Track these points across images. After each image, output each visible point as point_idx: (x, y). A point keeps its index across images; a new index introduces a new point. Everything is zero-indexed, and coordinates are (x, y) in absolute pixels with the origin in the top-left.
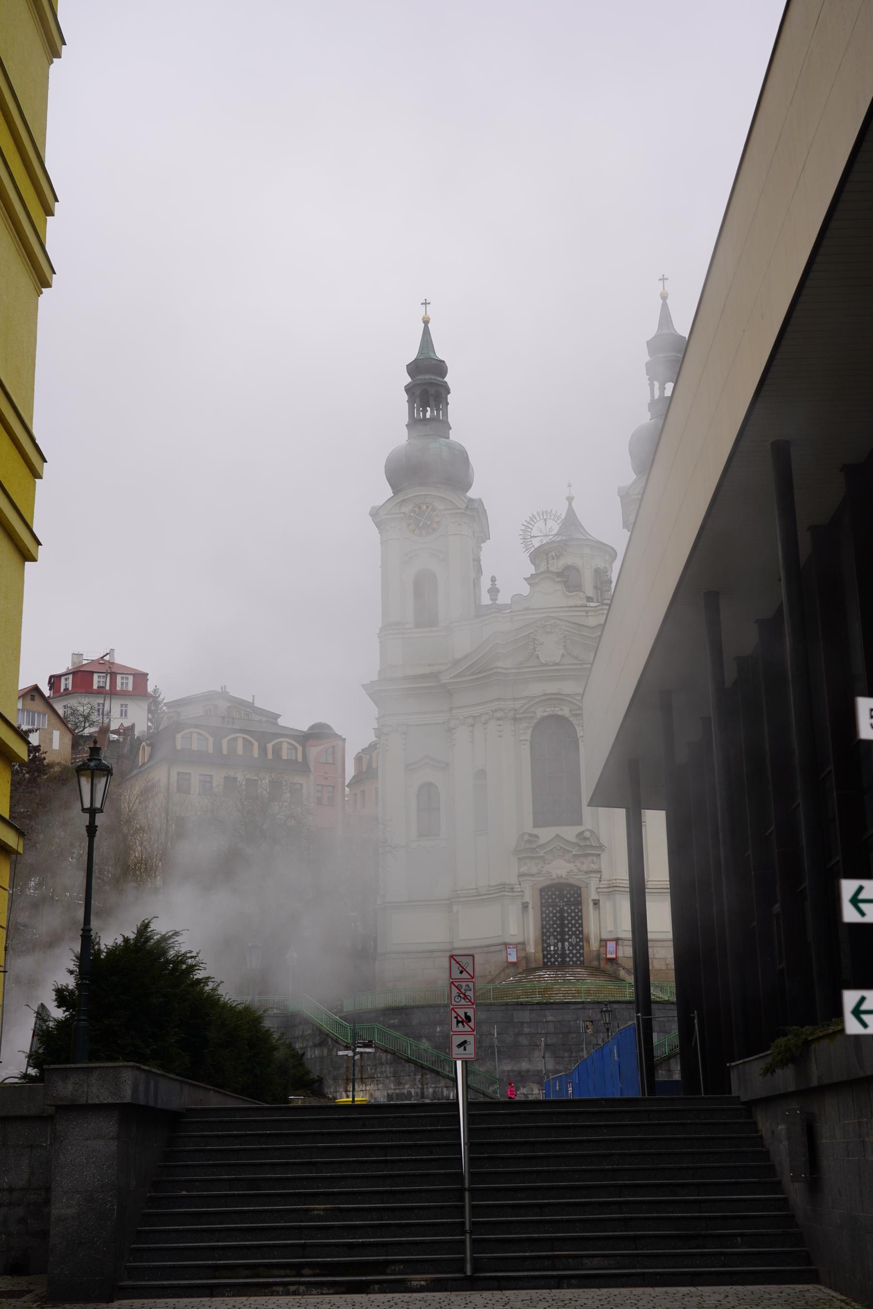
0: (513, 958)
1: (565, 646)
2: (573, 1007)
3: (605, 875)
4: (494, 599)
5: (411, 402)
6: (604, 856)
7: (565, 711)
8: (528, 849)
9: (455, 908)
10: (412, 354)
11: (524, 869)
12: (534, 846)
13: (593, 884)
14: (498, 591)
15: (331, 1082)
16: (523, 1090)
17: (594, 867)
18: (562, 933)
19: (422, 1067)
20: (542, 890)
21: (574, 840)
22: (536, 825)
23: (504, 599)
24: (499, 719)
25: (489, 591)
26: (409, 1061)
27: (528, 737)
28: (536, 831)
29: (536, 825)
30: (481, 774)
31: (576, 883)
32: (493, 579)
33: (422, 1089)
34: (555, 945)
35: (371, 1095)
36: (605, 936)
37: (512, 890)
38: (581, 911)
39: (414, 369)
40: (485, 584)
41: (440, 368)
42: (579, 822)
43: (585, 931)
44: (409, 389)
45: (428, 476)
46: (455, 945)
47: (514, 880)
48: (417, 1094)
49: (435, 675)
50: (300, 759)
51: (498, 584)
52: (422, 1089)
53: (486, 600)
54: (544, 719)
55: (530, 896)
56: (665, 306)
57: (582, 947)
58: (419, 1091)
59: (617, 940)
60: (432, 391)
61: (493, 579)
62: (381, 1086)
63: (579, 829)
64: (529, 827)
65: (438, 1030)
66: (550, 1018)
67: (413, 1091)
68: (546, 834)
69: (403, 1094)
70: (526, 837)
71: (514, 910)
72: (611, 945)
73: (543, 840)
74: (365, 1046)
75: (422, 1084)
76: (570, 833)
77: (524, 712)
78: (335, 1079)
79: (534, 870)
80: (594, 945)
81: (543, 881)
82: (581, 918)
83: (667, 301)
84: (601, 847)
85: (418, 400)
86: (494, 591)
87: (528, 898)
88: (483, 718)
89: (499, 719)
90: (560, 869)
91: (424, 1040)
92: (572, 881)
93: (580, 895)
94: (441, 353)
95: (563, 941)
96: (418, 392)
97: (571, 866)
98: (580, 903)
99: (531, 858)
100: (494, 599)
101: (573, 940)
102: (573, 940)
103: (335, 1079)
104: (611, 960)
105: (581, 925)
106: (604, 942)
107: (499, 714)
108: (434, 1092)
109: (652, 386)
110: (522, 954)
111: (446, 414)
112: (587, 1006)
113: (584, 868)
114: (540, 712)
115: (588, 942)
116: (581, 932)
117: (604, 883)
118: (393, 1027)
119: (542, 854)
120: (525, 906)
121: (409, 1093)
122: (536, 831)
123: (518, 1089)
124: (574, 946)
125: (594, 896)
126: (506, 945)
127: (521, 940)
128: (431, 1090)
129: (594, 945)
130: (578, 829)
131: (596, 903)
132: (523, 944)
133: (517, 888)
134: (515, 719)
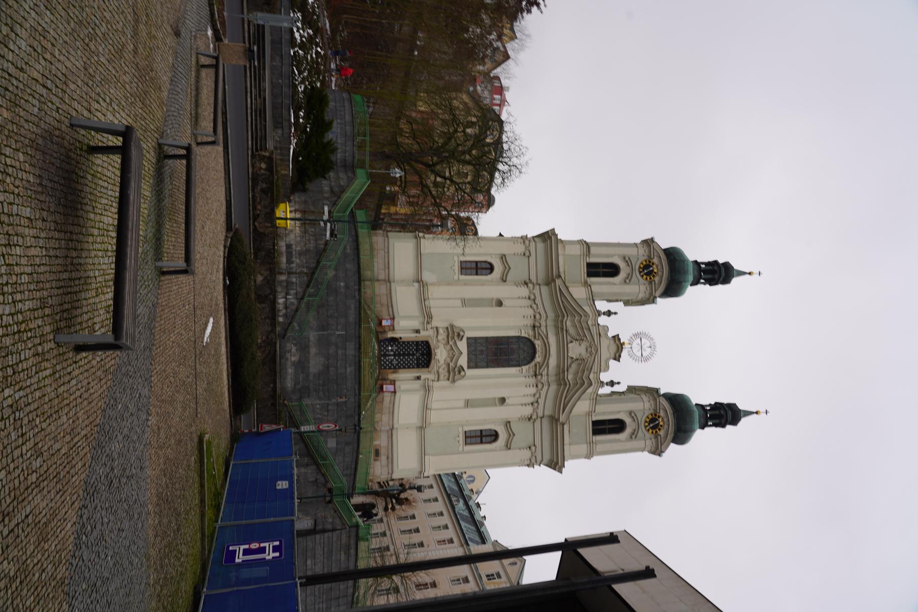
0: (384, 323)
1: (577, 359)
2: (357, 387)
3: (436, 384)
4: (604, 313)
5: (708, 264)
6: (447, 383)
7: (538, 359)
8: (454, 333)
9: (416, 285)
10: (737, 266)
11: (441, 331)
12: (456, 338)
13: (431, 376)
14: (609, 316)
15: (303, 198)
16: (294, 349)
17: (442, 377)
18: (399, 355)
19: (313, 273)
20: (427, 342)
21: (458, 364)
22: (468, 339)
23: (603, 320)
24: (535, 317)
25: (609, 311)
26: (318, 262)
27: (523, 335)
28: (465, 339)
29: (468, 339)
30: (500, 303)
31: (431, 365)
32: (615, 313)
33: (296, 273)
34: (392, 350)
35: (291, 231)
36: (397, 383)
37: (428, 323)
38: (413, 367)
39: (727, 267)
40: (612, 306)
41: (726, 280)
42: (469, 367)
43: (401, 371)
44: (716, 262)
45: (670, 273)
46: (392, 284)
47: (435, 323)
48: (291, 268)
49: (559, 276)
51: (613, 316)
52: (296, 273)
53: (602, 306)
55: (424, 335)
56: (751, 413)
57: (390, 368)
58: (294, 270)
59: (395, 392)
60: (716, 276)
61: (615, 313)
62: (299, 239)
63: (465, 367)
64: (469, 334)
65: (342, 284)
66: (348, 370)
67: (294, 265)
68: (463, 346)
69: (292, 257)
70: (462, 333)
71: (416, 324)
72: (391, 388)
73: (459, 343)
74: (332, 232)
75: (299, 273)
76: (463, 361)
77: (539, 334)
78: (305, 202)
79: (440, 338)
80: (392, 376)
81: (433, 344)
82: (409, 367)
83: (755, 415)
84: (454, 381)
85: (711, 268)
86: (609, 313)
87: (423, 333)
88: (534, 306)
89: (535, 317)
90: (441, 354)
91: (334, 273)
92: (433, 362)
93: (423, 367)
94: (735, 281)
95: (394, 355)
96: (716, 268)
97: (442, 362)
98: (418, 367)
99: (448, 336)
100: (604, 313)
101: (395, 362)
102: (395, 362)
103: (305, 202)
104: (382, 388)
105: (404, 368)
106: (393, 382)
107: (538, 316)
108: (293, 283)
109: (710, 405)
110: (387, 329)
112: (357, 398)
113: (441, 370)
114: (538, 343)
115: (394, 372)
116: (400, 368)
117: (431, 383)
118: (345, 248)
119: (451, 343)
120: (418, 331)
121: (292, 262)
122: (465, 339)
123: (295, 345)
124: (391, 363)
125: (423, 377)
126: (393, 319)
127: (396, 328)
128: (294, 280)
129: (392, 376)
130: (465, 367)
131: (418, 378)
132: (394, 329)
133: (429, 326)
134: (534, 327)
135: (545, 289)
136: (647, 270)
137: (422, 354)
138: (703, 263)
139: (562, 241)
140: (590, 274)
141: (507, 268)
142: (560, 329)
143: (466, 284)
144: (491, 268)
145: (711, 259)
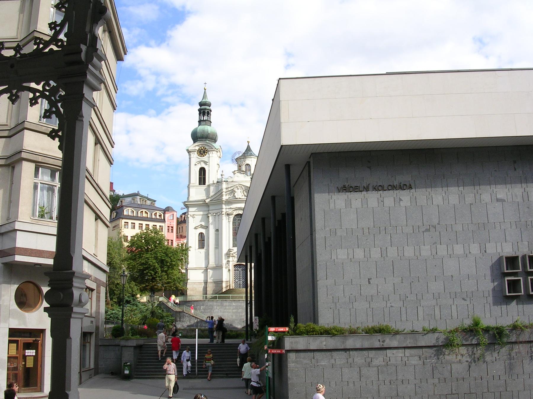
5: (200, 114)
9: (208, 270)
44: (199, 110)
50: (163, 218)
54: (236, 215)
60: (206, 111)
111: (210, 118)
114: (235, 213)
120: (229, 270)
135: (211, 208)
136: (202, 152)
137: (240, 268)
138: (200, 118)
139: (188, 198)
140: (204, 184)
141: (202, 227)
142: (228, 202)
143: (208, 246)
144: (202, 233)
145: (198, 112)
